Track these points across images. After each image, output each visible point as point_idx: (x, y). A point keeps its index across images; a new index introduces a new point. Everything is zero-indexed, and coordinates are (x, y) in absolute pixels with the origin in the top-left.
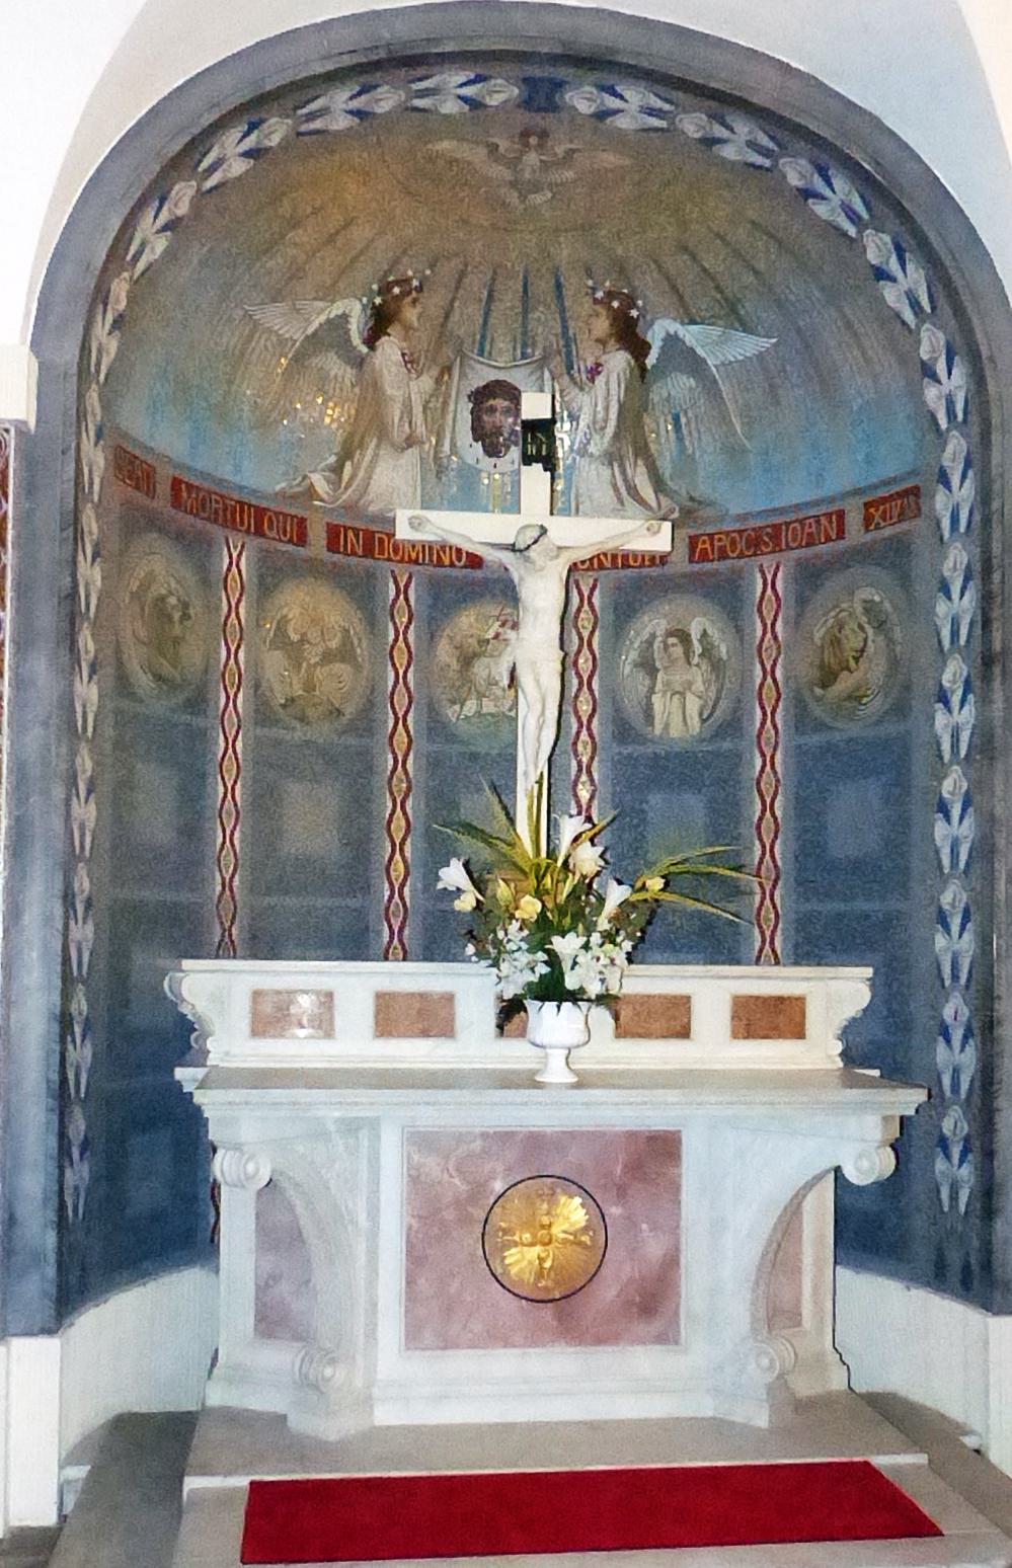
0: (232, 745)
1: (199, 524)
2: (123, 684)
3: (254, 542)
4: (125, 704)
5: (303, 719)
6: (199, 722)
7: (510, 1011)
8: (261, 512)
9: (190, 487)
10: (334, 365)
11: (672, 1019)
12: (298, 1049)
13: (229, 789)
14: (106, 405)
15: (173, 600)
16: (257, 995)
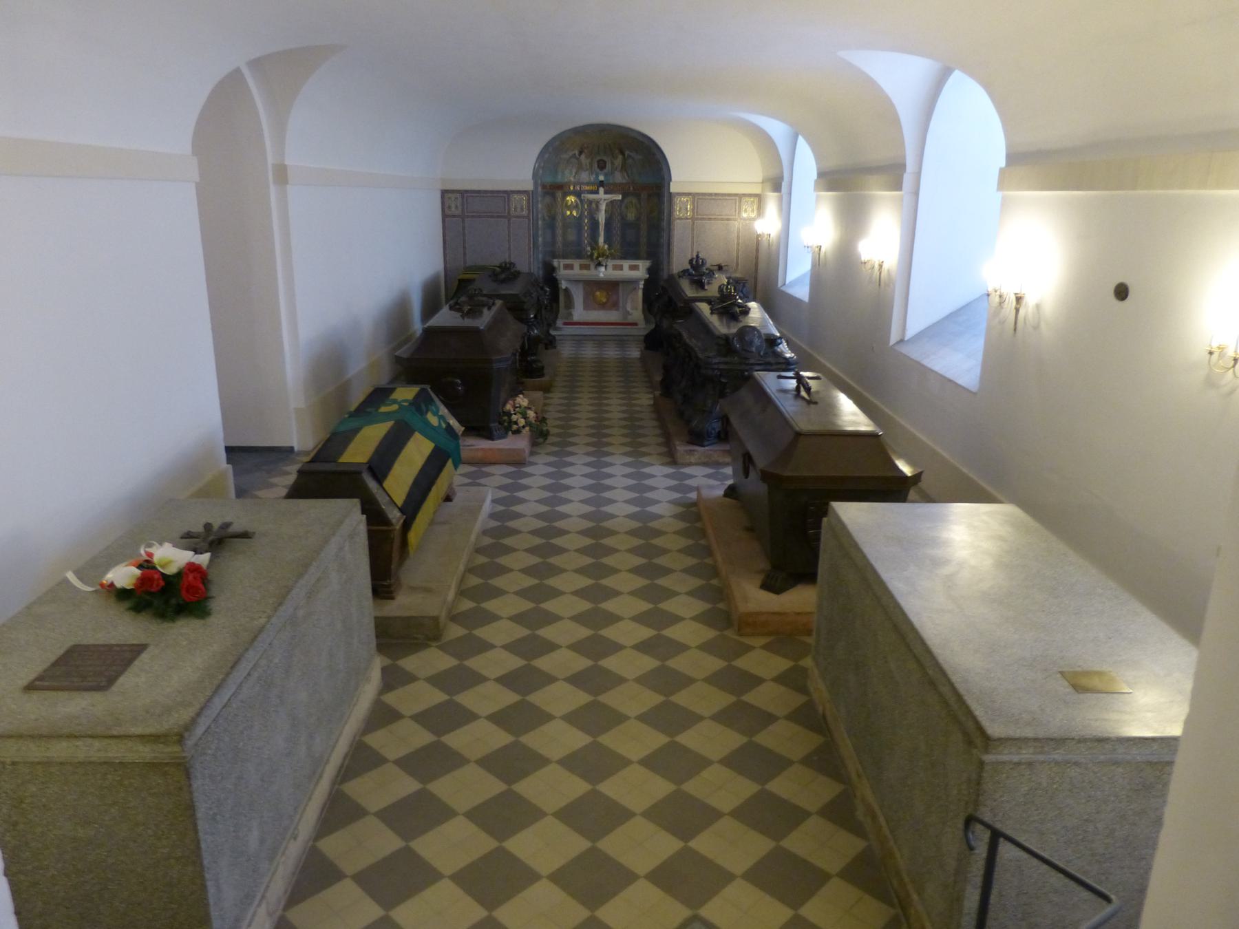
0: (559, 224)
10: (574, 160)
11: (621, 268)
13: (559, 232)
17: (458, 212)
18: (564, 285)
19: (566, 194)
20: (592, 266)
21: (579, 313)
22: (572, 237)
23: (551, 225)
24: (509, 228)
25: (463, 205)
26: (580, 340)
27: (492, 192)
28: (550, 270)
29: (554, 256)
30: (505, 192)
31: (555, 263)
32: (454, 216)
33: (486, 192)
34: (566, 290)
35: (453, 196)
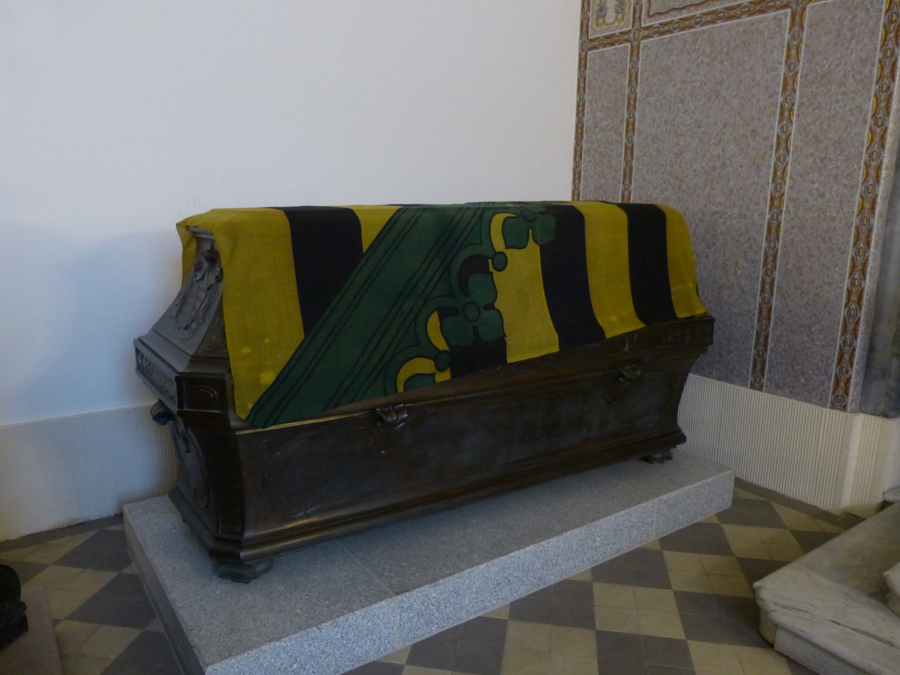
24: (793, 50)
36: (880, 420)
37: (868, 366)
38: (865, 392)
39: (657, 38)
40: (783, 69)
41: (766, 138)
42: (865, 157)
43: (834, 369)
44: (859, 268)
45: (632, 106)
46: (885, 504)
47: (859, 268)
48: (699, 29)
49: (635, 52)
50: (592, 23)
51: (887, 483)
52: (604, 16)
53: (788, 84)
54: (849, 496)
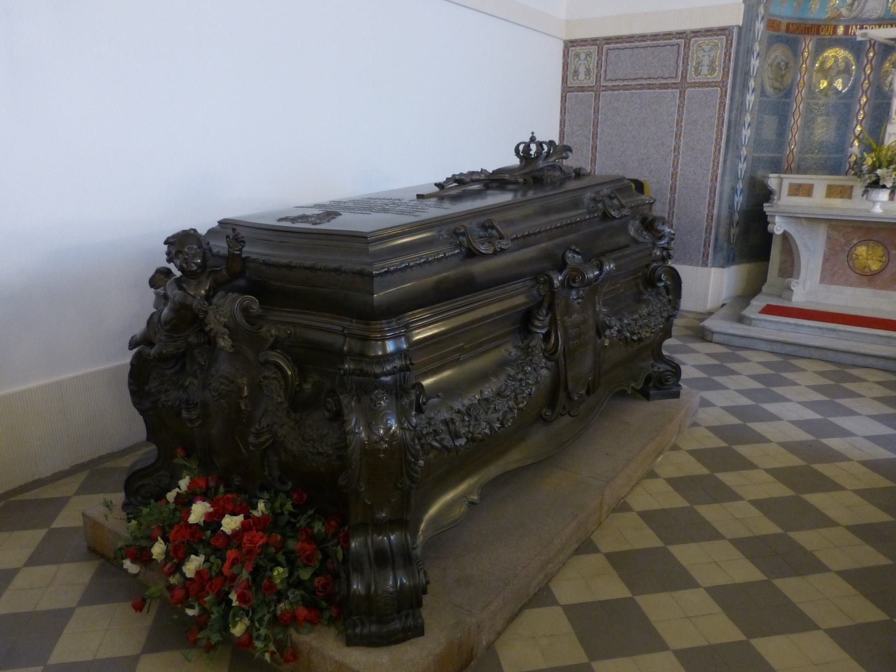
0: (799, 106)
1: (795, 36)
2: (763, 93)
3: (815, 37)
4: (764, 99)
5: (826, 95)
6: (788, 100)
7: (866, 192)
8: (819, 26)
9: (793, 24)
12: (800, 201)
13: (796, 121)
14: (766, 8)
15: (782, 63)
16: (791, 185)
17: (591, 82)
18: (778, 227)
19: (820, 48)
20: (858, 190)
21: (807, 289)
22: (823, 131)
23: (780, 105)
24: (681, 107)
25: (599, 66)
26: (789, 355)
27: (655, 37)
28: (760, 195)
29: (777, 167)
30: (681, 34)
31: (773, 181)
32: (582, 89)
33: (643, 37)
34: (785, 236)
35: (582, 51)
36: (721, 269)
37: (715, 247)
38: (714, 258)
39: (610, 92)
40: (676, 116)
41: (669, 147)
42: (712, 158)
43: (702, 249)
44: (711, 205)
45: (596, 125)
46: (723, 305)
47: (711, 205)
48: (633, 91)
49: (597, 97)
50: (570, 78)
51: (723, 298)
52: (578, 76)
53: (679, 123)
54: (710, 305)
